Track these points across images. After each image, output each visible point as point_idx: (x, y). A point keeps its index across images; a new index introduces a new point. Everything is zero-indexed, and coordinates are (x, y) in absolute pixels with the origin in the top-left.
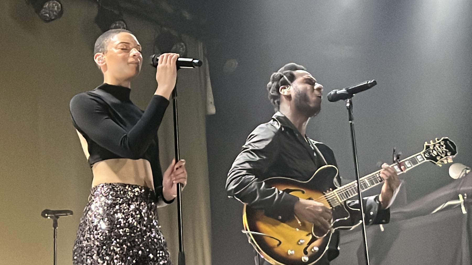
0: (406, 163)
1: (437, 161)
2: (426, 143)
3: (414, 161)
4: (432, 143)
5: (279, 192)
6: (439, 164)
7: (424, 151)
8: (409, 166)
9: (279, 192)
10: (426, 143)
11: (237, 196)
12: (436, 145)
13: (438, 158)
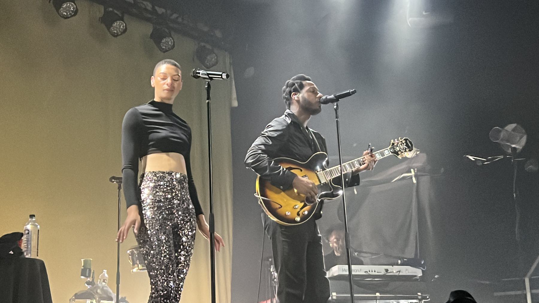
0: (377, 155)
1: (398, 155)
2: (392, 141)
3: (382, 154)
4: (396, 142)
5: (283, 169)
6: (400, 157)
7: (390, 147)
8: (378, 157)
9: (283, 169)
10: (392, 141)
11: (253, 168)
12: (399, 143)
13: (399, 153)
